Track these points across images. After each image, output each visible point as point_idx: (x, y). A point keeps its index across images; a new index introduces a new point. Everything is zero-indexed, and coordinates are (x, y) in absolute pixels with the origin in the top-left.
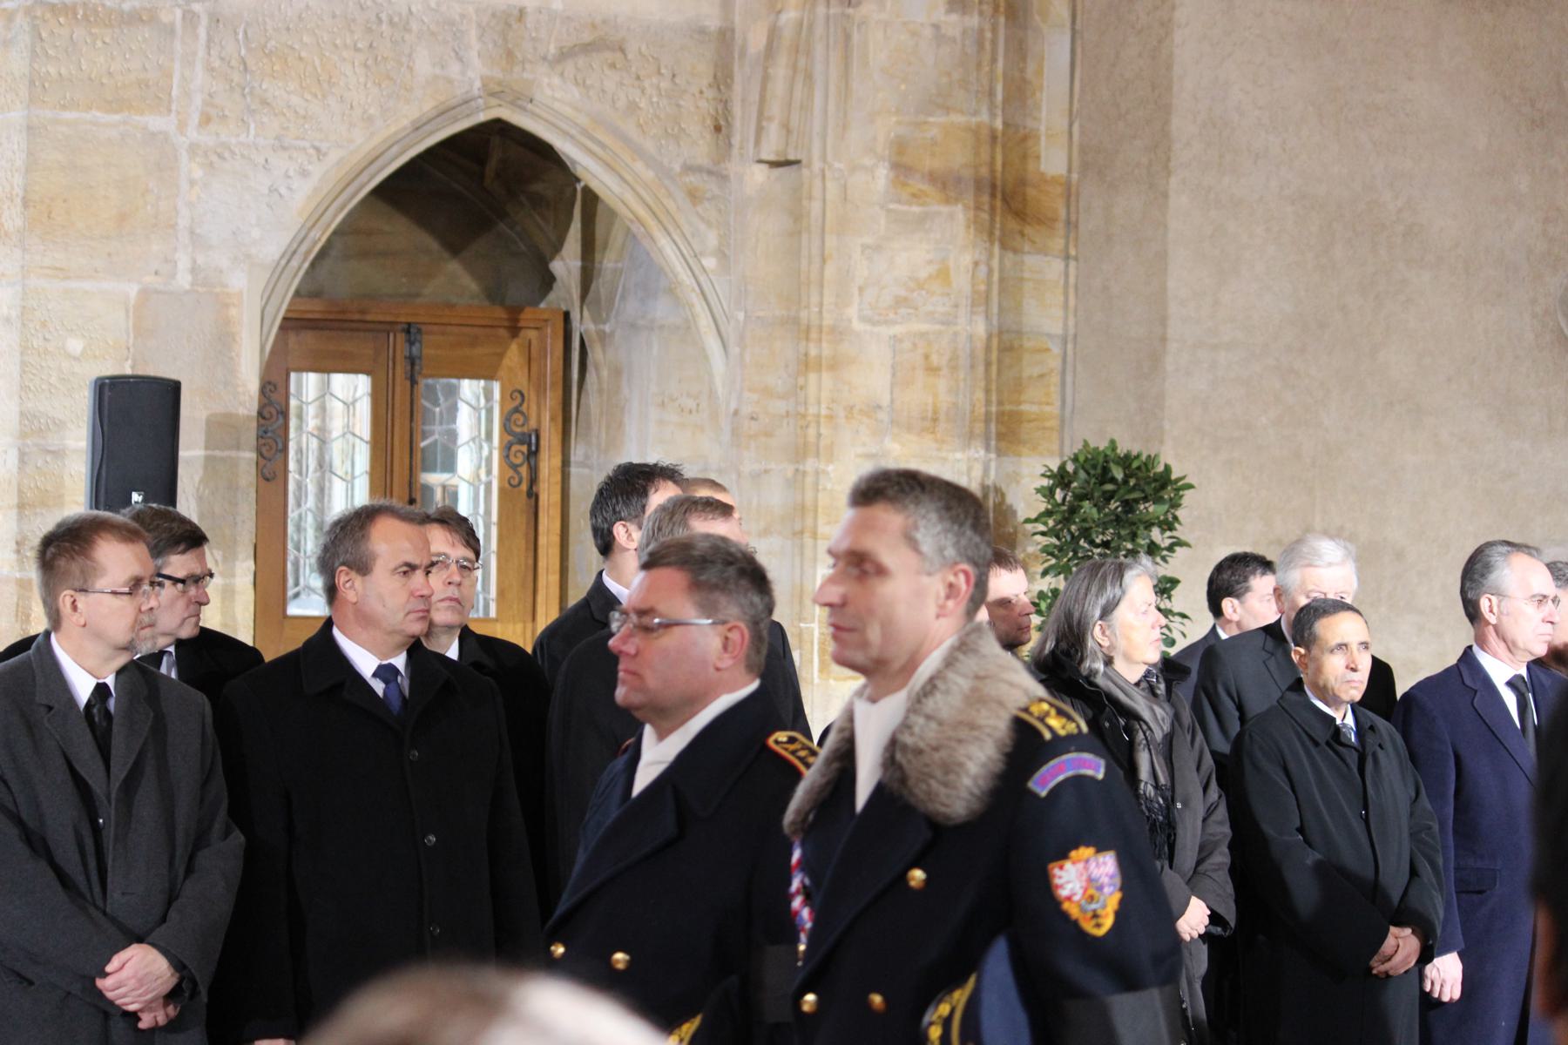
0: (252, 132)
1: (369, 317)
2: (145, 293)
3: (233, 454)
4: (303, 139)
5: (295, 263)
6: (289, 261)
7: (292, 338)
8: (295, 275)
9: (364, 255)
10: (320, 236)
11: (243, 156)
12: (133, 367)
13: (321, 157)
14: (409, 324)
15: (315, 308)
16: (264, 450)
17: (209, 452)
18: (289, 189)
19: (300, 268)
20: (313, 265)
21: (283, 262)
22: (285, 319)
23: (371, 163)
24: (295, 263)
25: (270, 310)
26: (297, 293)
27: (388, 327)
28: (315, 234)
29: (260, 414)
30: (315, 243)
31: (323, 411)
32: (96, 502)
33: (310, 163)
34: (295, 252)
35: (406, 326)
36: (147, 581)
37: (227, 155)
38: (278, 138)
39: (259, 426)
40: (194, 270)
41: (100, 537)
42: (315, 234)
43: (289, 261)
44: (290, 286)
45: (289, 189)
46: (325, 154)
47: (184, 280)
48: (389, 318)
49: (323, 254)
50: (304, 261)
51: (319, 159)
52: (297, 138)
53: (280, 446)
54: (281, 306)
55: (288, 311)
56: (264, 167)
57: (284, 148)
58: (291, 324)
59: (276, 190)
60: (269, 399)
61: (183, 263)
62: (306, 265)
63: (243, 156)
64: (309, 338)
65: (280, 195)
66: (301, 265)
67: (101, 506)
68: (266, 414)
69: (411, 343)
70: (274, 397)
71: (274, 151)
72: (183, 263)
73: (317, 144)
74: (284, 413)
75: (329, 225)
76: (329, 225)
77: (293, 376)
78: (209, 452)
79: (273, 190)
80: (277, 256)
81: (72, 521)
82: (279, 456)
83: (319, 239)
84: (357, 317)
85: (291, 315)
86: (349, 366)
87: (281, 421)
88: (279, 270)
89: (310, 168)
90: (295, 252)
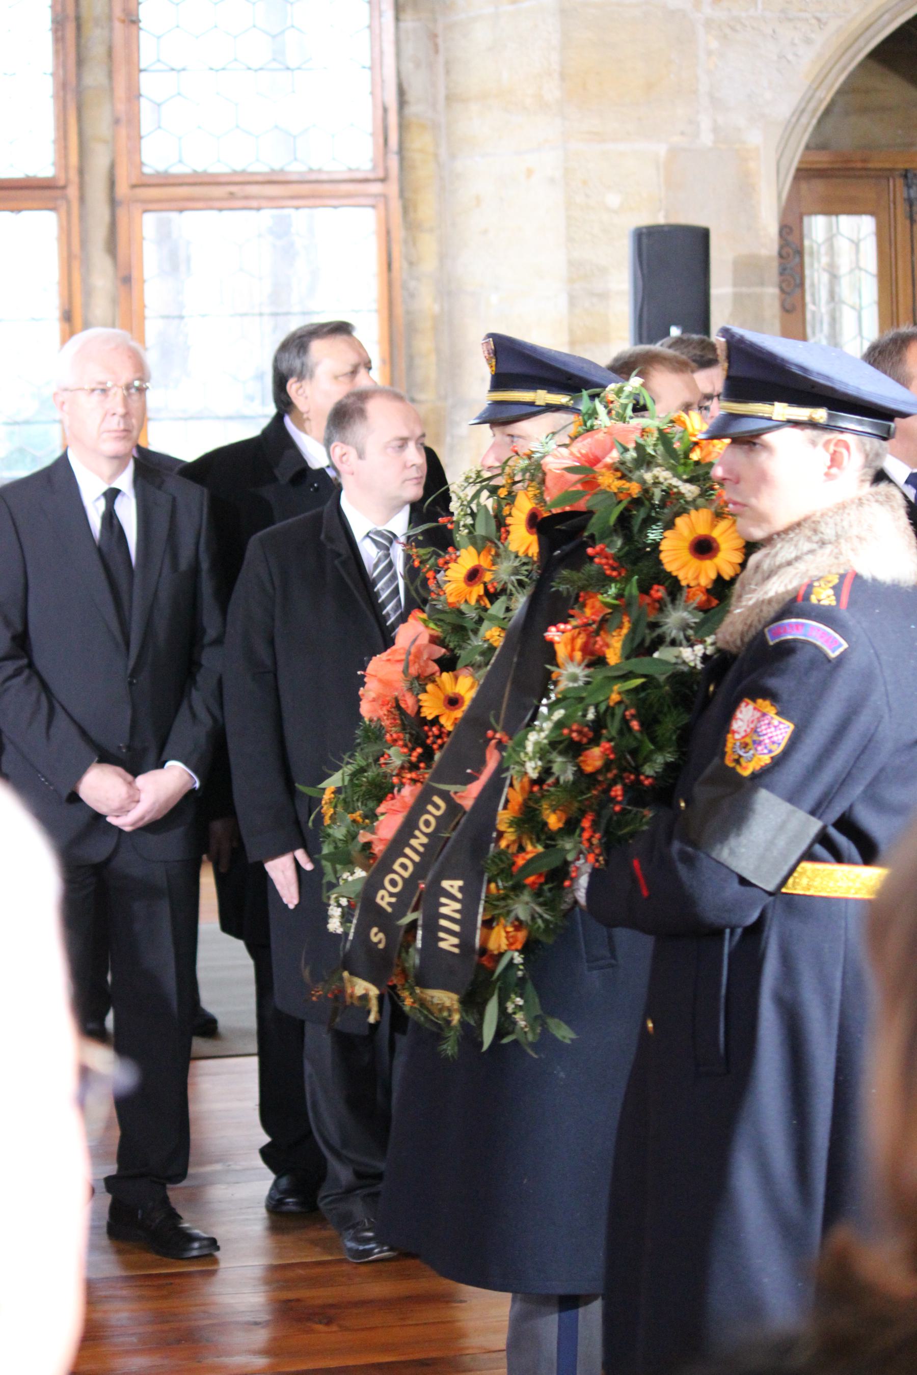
0: (760, 6)
1: (870, 165)
2: (674, 152)
3: (757, 290)
4: (805, 11)
5: (804, 120)
6: (798, 119)
7: (804, 186)
8: (805, 131)
9: (864, 110)
10: (826, 95)
11: (753, 28)
12: (666, 217)
13: (822, 26)
14: (906, 171)
15: (822, 159)
16: (784, 285)
17: (744, 290)
18: (796, 55)
19: (808, 124)
20: (820, 122)
21: (794, 120)
22: (798, 170)
23: (867, 29)
24: (804, 120)
25: (785, 162)
26: (807, 147)
27: (885, 174)
28: (820, 94)
29: (781, 256)
30: (821, 101)
31: (832, 251)
32: (640, 338)
33: (812, 31)
34: (803, 111)
35: (904, 173)
36: (696, 406)
37: (738, 27)
38: (783, 11)
39: (781, 264)
40: (716, 129)
41: (654, 368)
42: (820, 94)
43: (798, 119)
44: (799, 142)
45: (796, 55)
46: (825, 24)
47: (706, 139)
48: (887, 165)
49: (828, 111)
50: (812, 117)
51: (820, 28)
52: (801, 10)
53: (798, 281)
54: (794, 157)
55: (801, 162)
56: (772, 37)
57: (790, 20)
58: (804, 173)
59: (784, 57)
60: (786, 240)
61: (705, 123)
62: (814, 121)
63: (753, 28)
64: (819, 186)
65: (789, 62)
66: (809, 122)
67: (644, 340)
68: (784, 253)
69: (909, 187)
70: (790, 238)
71: (780, 22)
72: (705, 123)
73: (818, 15)
74: (800, 252)
75: (832, 85)
76: (832, 85)
77: (806, 219)
78: (744, 290)
79: (781, 57)
80: (788, 115)
81: (628, 355)
82: (798, 291)
83: (825, 98)
84: (859, 165)
85: (804, 166)
86: (853, 208)
87: (797, 260)
88: (791, 127)
89: (813, 36)
90: (803, 111)
